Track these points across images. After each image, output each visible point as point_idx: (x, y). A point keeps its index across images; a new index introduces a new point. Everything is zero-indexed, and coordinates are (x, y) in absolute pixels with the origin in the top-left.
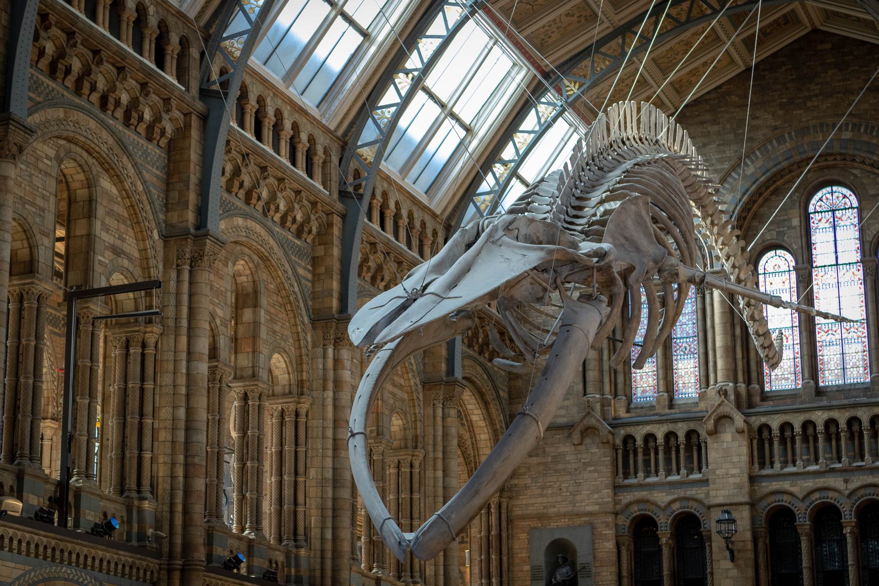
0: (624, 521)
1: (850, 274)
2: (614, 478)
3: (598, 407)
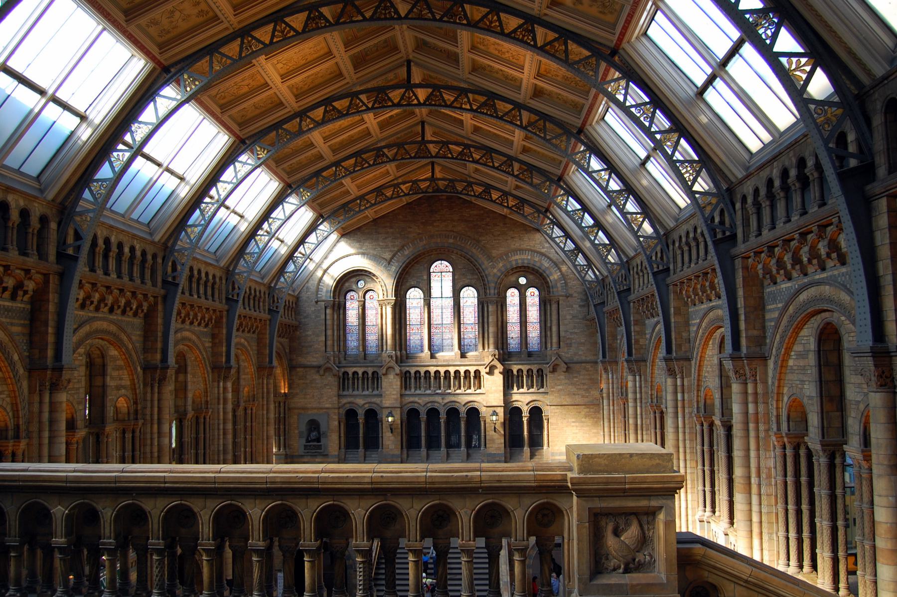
0: (343, 411)
1: (447, 303)
3: (332, 358)
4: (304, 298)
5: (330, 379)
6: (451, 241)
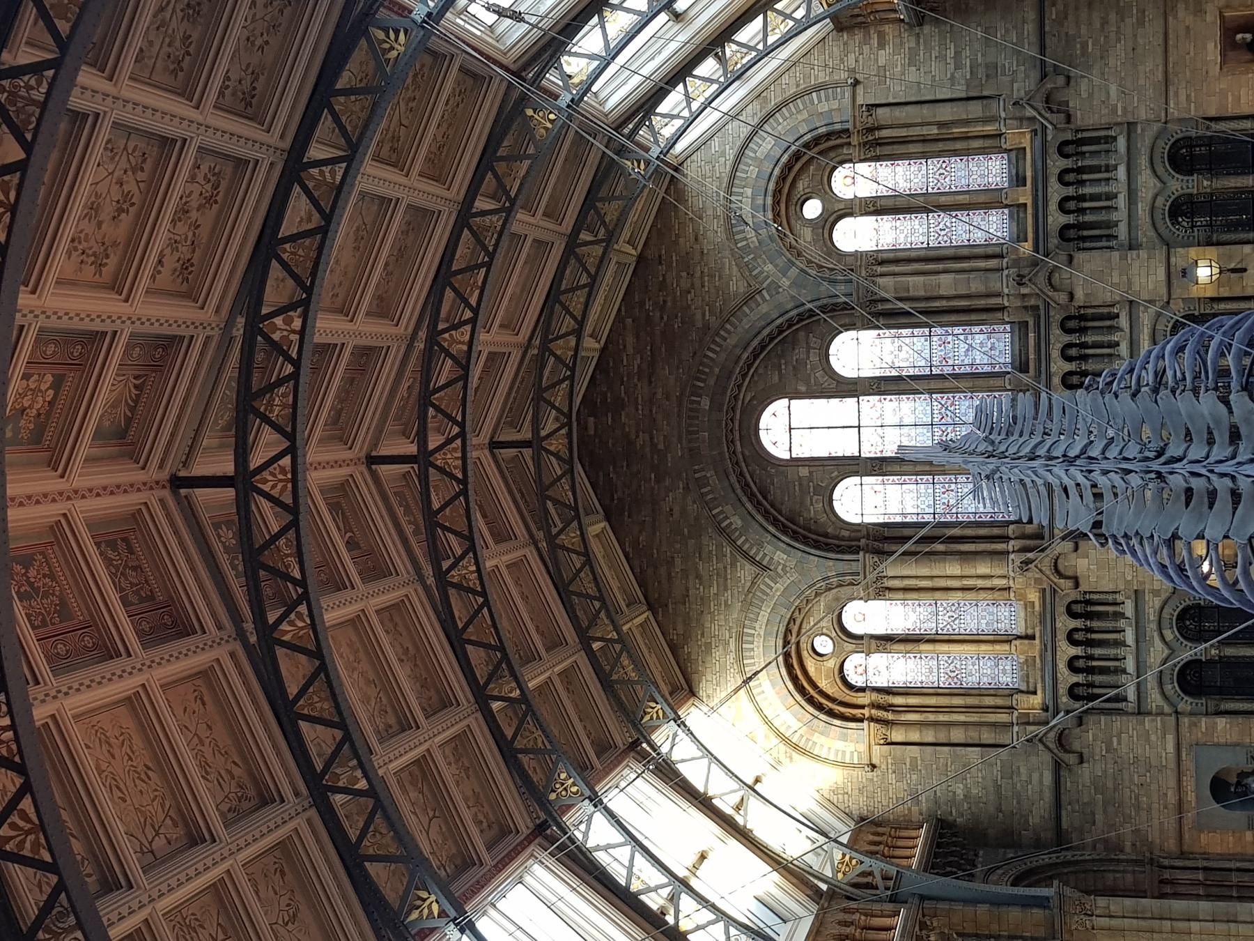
0: (1186, 704)
2: (1127, 713)
4: (862, 800)
5: (1092, 735)
6: (705, 403)
